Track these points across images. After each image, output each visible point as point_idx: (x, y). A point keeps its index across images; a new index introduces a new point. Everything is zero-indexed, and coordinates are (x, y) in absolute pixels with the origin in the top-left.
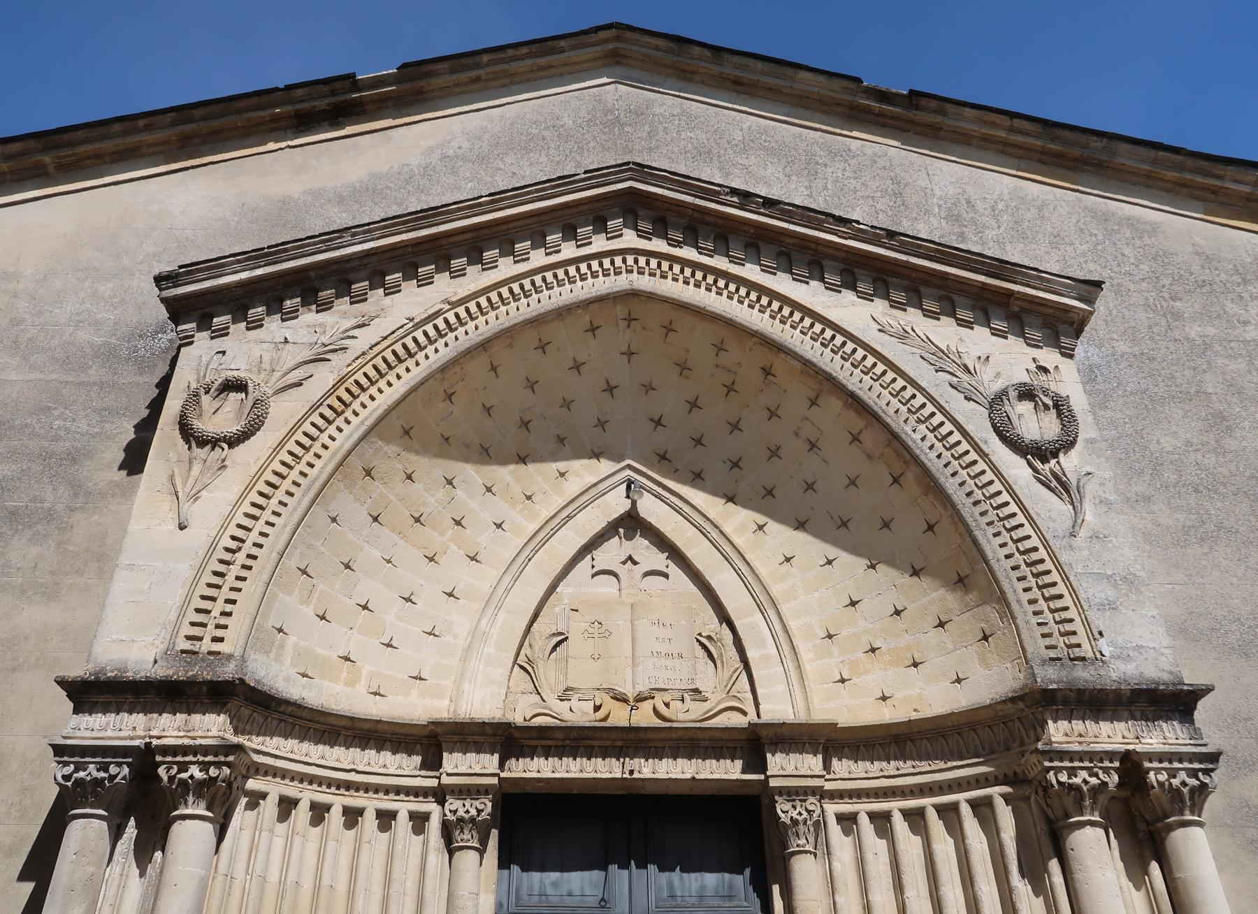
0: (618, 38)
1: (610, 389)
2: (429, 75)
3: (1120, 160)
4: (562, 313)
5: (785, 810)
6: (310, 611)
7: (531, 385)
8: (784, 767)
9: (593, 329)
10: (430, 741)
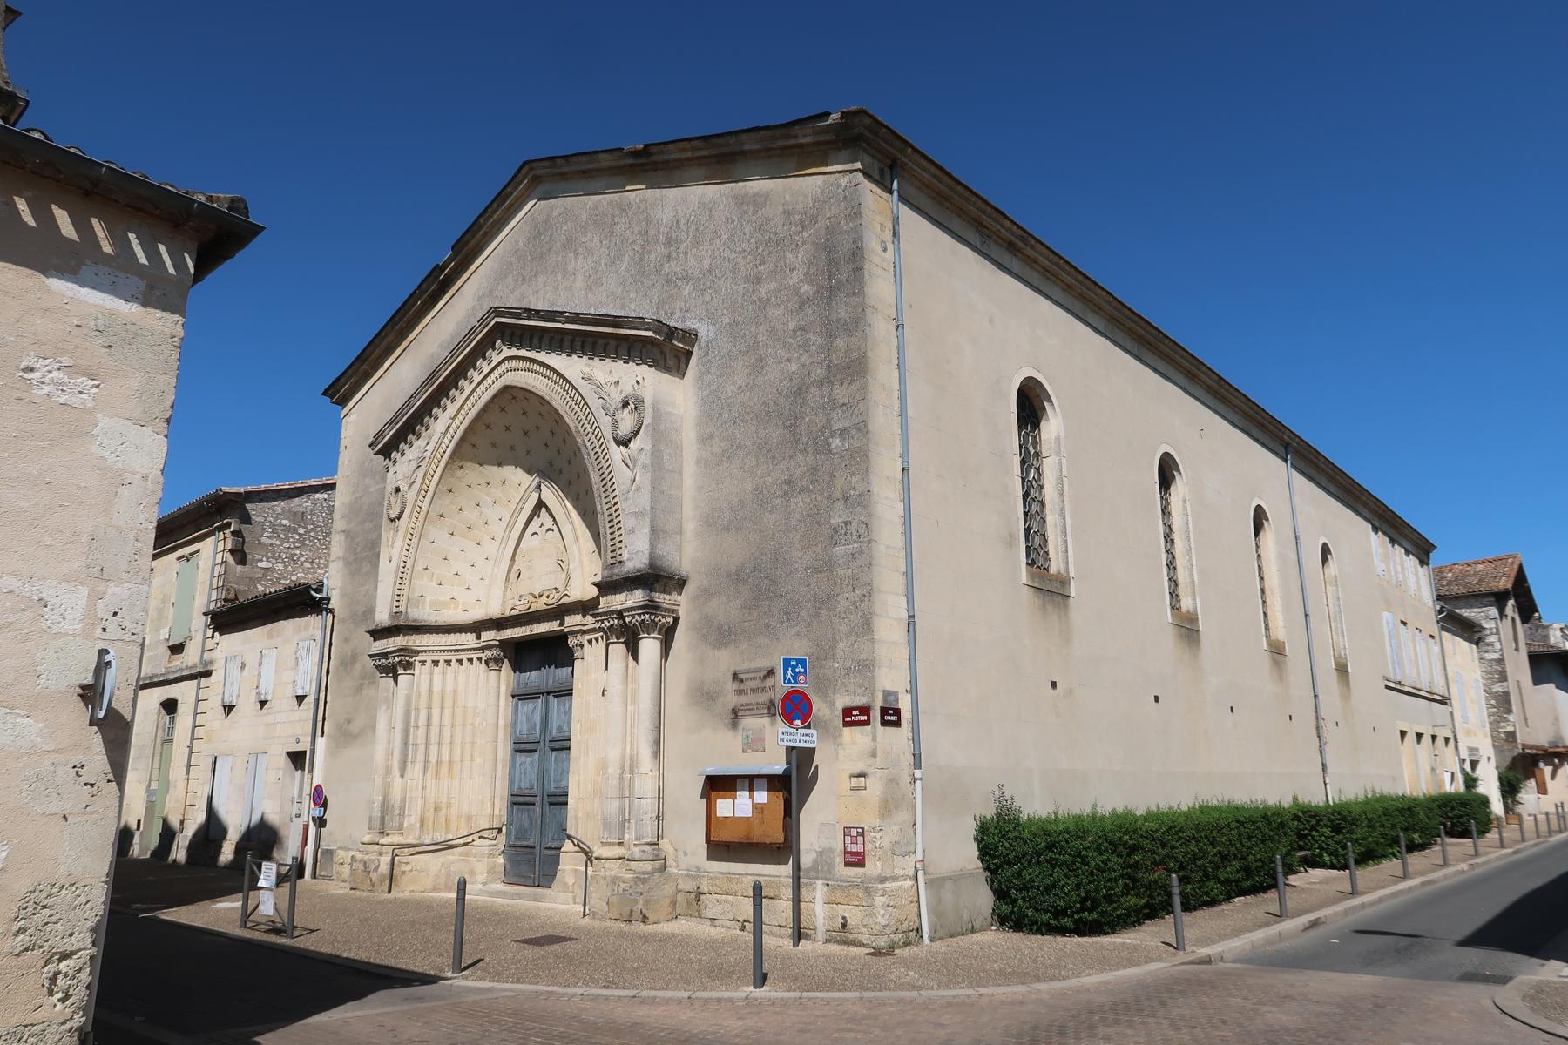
1: (526, 434)
2: (467, 243)
3: (746, 147)
4: (485, 409)
5: (572, 642)
7: (494, 445)
8: (573, 621)
10: (477, 627)
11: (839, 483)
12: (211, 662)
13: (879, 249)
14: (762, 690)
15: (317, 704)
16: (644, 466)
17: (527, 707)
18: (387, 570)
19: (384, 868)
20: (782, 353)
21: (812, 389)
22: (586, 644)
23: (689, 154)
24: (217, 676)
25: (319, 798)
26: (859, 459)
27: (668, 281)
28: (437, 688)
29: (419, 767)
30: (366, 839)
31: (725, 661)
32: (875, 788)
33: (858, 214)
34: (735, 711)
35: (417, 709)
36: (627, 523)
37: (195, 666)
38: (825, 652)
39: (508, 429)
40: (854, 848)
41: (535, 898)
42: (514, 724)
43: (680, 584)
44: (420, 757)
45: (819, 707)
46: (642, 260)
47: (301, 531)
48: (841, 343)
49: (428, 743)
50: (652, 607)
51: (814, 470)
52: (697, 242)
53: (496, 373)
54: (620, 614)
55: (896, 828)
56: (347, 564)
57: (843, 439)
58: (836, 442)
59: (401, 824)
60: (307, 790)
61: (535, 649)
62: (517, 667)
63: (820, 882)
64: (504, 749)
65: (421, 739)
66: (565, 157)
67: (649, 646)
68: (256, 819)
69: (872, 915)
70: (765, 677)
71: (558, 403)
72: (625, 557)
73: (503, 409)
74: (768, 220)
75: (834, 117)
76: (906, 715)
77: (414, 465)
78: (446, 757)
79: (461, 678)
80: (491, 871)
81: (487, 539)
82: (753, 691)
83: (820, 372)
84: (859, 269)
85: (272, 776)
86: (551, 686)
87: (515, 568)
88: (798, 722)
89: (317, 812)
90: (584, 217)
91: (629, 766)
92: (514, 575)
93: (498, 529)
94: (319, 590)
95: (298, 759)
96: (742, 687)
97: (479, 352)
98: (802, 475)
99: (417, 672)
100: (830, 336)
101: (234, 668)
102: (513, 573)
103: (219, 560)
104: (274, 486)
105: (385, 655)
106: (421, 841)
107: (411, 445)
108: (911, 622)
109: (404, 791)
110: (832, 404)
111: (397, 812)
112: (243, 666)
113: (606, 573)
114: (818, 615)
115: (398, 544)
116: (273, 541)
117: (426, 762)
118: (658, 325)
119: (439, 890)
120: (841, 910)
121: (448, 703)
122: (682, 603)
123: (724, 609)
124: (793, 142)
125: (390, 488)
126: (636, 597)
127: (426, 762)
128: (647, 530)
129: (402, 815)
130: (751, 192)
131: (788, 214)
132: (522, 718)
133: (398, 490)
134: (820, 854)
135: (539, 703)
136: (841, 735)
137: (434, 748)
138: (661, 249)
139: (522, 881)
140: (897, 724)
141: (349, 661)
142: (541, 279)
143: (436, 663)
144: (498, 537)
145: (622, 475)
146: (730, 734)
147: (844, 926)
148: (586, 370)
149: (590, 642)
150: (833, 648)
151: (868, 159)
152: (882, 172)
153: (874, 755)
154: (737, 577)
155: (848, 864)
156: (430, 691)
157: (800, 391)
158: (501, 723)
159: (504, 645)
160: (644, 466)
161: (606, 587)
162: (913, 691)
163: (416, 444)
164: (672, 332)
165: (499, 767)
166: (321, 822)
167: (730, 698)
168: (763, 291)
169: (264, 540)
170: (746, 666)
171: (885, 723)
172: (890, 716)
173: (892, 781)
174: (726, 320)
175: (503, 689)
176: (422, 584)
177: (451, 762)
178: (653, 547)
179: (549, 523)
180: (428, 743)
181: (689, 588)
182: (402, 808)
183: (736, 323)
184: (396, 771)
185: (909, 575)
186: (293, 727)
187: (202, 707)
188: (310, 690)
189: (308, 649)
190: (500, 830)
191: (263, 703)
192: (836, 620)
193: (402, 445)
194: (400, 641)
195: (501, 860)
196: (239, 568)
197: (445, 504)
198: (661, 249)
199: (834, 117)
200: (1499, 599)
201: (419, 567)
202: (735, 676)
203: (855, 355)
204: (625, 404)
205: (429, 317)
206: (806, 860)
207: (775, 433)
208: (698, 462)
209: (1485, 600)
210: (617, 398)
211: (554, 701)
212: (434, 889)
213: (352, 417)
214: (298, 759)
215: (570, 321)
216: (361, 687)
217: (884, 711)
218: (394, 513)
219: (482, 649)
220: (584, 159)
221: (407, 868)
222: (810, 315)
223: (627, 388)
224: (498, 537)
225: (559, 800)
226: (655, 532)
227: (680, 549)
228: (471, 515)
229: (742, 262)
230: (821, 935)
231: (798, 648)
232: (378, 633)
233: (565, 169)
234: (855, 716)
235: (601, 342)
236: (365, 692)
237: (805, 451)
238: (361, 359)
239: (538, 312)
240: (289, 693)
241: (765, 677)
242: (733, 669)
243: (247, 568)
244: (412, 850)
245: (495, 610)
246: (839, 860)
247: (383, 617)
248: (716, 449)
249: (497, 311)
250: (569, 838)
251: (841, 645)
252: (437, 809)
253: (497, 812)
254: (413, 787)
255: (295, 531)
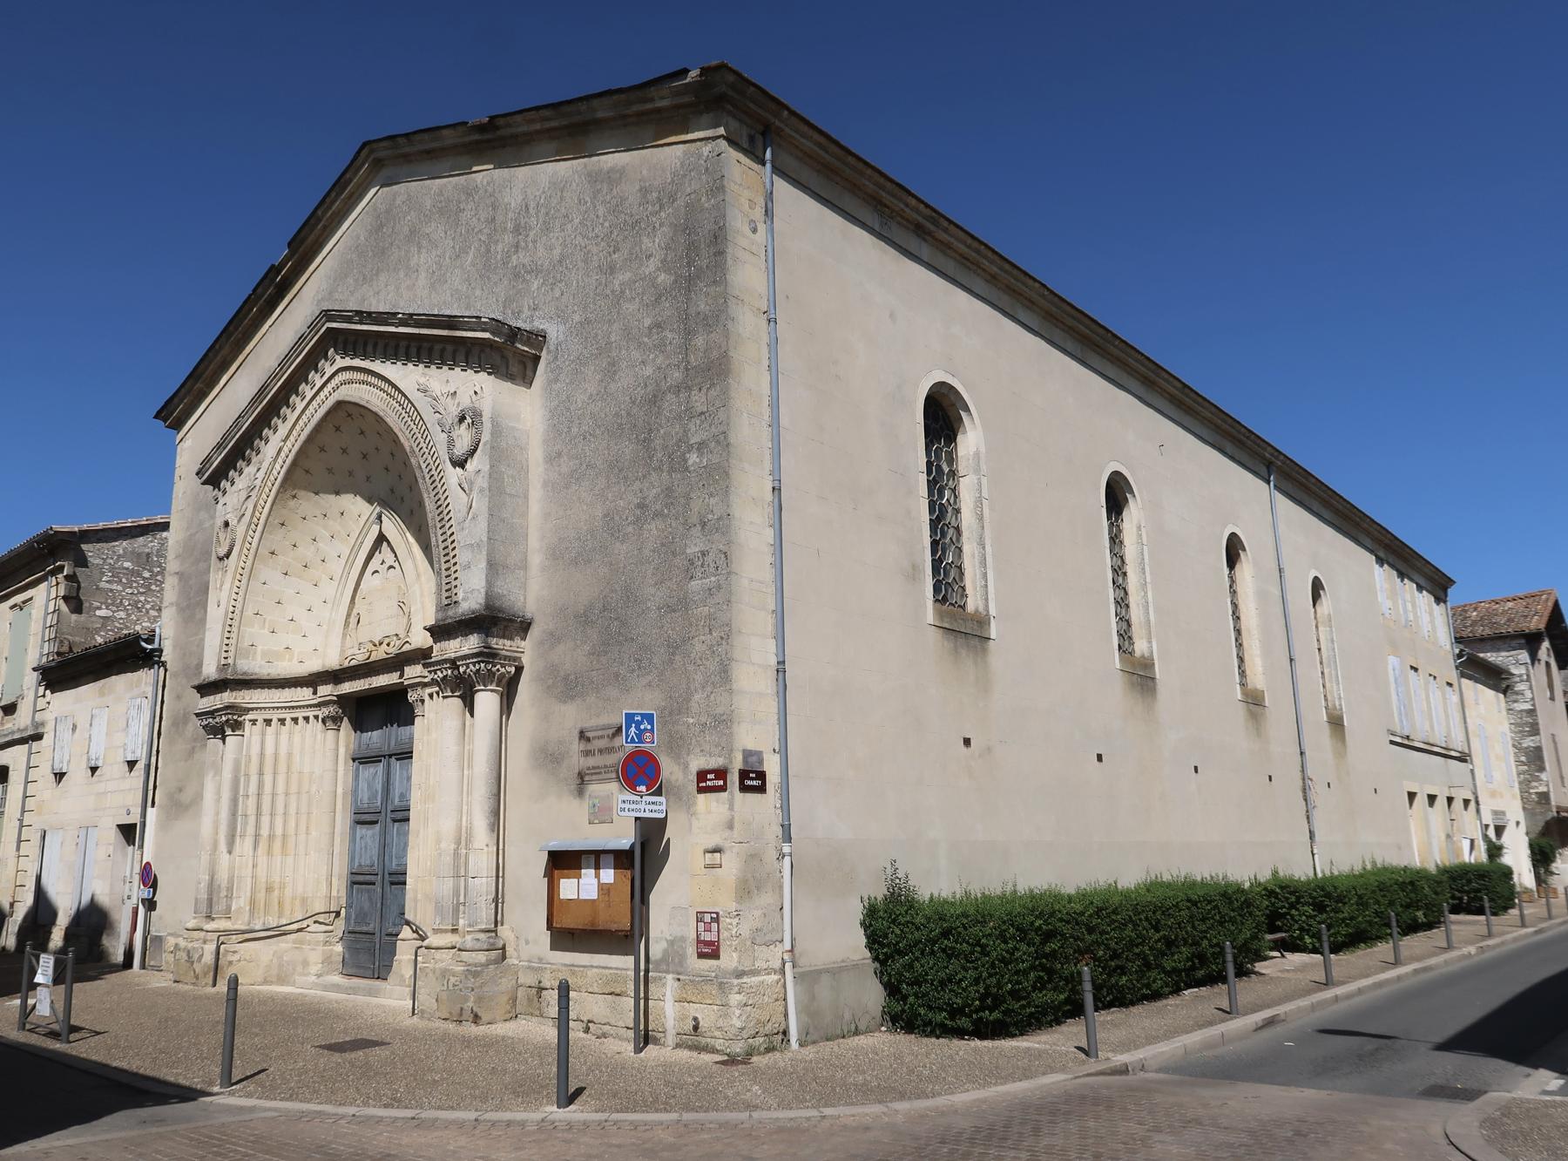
0: (372, 151)
1: (365, 456)
5: (412, 696)
6: (266, 631)
7: (330, 470)
8: (414, 672)
9: (338, 429)
10: (313, 681)
11: (696, 506)
12: (43, 724)
13: (747, 230)
14: (610, 750)
15: (147, 769)
16: (481, 490)
17: (368, 771)
18: (215, 615)
19: (209, 958)
20: (636, 355)
21: (669, 396)
22: (427, 698)
23: (538, 126)
24: (47, 740)
25: (149, 878)
26: (719, 477)
27: (517, 276)
28: (269, 750)
29: (249, 841)
30: (190, 925)
31: (571, 717)
32: (731, 865)
33: (721, 189)
34: (581, 776)
35: (247, 775)
36: (463, 556)
37: (26, 729)
38: (677, 707)
39: (344, 451)
40: (707, 937)
41: (371, 993)
42: (355, 791)
43: (524, 627)
44: (251, 830)
45: (669, 770)
46: (488, 251)
47: (147, 574)
48: (699, 341)
49: (259, 814)
50: (488, 655)
51: (669, 491)
52: (547, 229)
53: (329, 387)
54: (453, 663)
55: (758, 913)
56: (181, 610)
57: (701, 455)
58: (693, 458)
59: (229, 908)
60: (137, 869)
61: (374, 706)
62: (359, 726)
63: (670, 977)
64: (343, 820)
65: (251, 810)
66: (407, 135)
67: (487, 701)
68: (86, 900)
69: (726, 1015)
70: (614, 735)
71: (392, 420)
72: (461, 595)
73: (338, 429)
74: (623, 199)
75: (694, 73)
76: (773, 778)
77: (244, 495)
78: (279, 831)
79: (297, 739)
80: (327, 960)
81: (325, 578)
82: (601, 751)
83: (678, 375)
84: (721, 253)
85: (101, 853)
86: (393, 748)
87: (355, 612)
88: (643, 788)
89: (146, 893)
90: (428, 203)
91: (463, 839)
92: (353, 620)
93: (336, 567)
94: (150, 640)
95: (129, 833)
96: (590, 747)
97: (311, 363)
98: (657, 497)
99: (247, 733)
100: (689, 333)
101: (65, 733)
102: (352, 618)
103: (51, 609)
104: (114, 524)
105: (212, 713)
106: (252, 926)
107: (241, 473)
108: (781, 669)
109: (232, 869)
110: (690, 413)
111: (224, 893)
112: (74, 728)
113: (440, 616)
114: (671, 662)
115: (227, 586)
116: (114, 587)
117: (257, 836)
118: (496, 325)
119: (271, 983)
120: (694, 1010)
121: (282, 767)
122: (526, 649)
123: (571, 656)
124: (649, 106)
125: (219, 522)
126: (468, 644)
127: (257, 836)
128: (483, 565)
129: (229, 897)
130: (606, 167)
131: (644, 191)
132: (363, 785)
133: (227, 524)
134: (671, 943)
135: (380, 767)
136: (695, 804)
137: (265, 820)
138: (508, 238)
139: (361, 972)
140: (761, 789)
141: (180, 722)
142: (383, 277)
143: (268, 722)
144: (337, 577)
145: (457, 501)
146: (576, 803)
147: (696, 1028)
148: (422, 380)
149: (431, 696)
150: (688, 700)
151: (734, 124)
152: (752, 139)
153: (730, 826)
154: (584, 619)
155: (701, 955)
156: (262, 754)
157: (654, 400)
158: (340, 790)
159: (342, 700)
160: (481, 490)
161: (440, 632)
162: (783, 751)
163: (246, 470)
164: (514, 334)
165: (337, 840)
166: (150, 905)
167: (576, 760)
168: (617, 282)
169: (102, 585)
170: (593, 722)
171: (744, 789)
172: (753, 780)
173: (753, 858)
174: (577, 318)
175: (342, 750)
176: (254, 632)
177: (284, 836)
178: (490, 584)
179: (390, 559)
180: (259, 814)
181: (534, 632)
182: (230, 889)
183: (589, 322)
184: (223, 847)
185: (780, 615)
186: (123, 797)
187: (33, 774)
188: (140, 754)
189: (140, 707)
190: (338, 914)
191: (94, 770)
192: (691, 668)
193: (231, 473)
194: (227, 697)
195: (339, 948)
196: (74, 617)
197: (277, 539)
198: (508, 238)
199: (694, 73)
200: (1530, 641)
201: (249, 612)
202: (582, 735)
203: (715, 354)
204: (462, 419)
205: (270, 322)
206: (656, 950)
207: (628, 449)
208: (545, 484)
209: (1514, 643)
210: (454, 411)
211: (396, 765)
212: (265, 982)
213: (187, 443)
214: (129, 833)
215: (403, 323)
216: (192, 751)
217: (744, 775)
218: (222, 551)
219: (319, 705)
220: (426, 136)
221: (235, 958)
222: (667, 309)
223: (465, 400)
224: (337, 577)
225: (398, 879)
226: (493, 567)
227: (524, 586)
228: (306, 551)
229: (595, 250)
230: (671, 1039)
231: (645, 700)
232: (206, 689)
233: (407, 150)
234: (710, 781)
235: (438, 347)
236: (196, 756)
237: (659, 469)
238: (194, 375)
239: (369, 314)
240: (120, 758)
241: (614, 735)
242: (579, 726)
243: (83, 618)
244: (241, 937)
245: (332, 659)
246: (691, 951)
247: (210, 671)
248: (565, 469)
249: (327, 315)
250: (408, 923)
251: (697, 697)
252: (269, 890)
253: (334, 893)
254: (242, 866)
255: (139, 575)
